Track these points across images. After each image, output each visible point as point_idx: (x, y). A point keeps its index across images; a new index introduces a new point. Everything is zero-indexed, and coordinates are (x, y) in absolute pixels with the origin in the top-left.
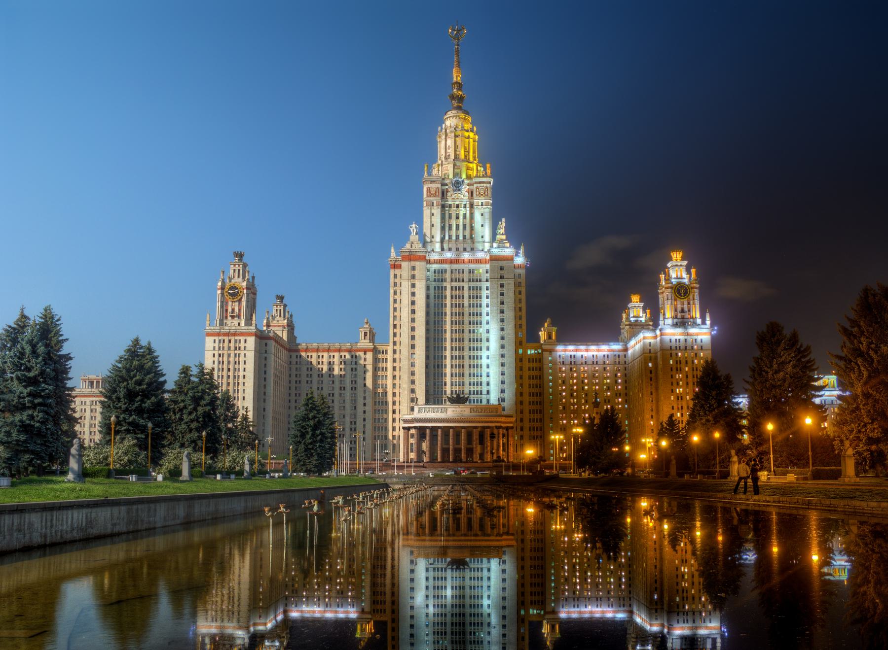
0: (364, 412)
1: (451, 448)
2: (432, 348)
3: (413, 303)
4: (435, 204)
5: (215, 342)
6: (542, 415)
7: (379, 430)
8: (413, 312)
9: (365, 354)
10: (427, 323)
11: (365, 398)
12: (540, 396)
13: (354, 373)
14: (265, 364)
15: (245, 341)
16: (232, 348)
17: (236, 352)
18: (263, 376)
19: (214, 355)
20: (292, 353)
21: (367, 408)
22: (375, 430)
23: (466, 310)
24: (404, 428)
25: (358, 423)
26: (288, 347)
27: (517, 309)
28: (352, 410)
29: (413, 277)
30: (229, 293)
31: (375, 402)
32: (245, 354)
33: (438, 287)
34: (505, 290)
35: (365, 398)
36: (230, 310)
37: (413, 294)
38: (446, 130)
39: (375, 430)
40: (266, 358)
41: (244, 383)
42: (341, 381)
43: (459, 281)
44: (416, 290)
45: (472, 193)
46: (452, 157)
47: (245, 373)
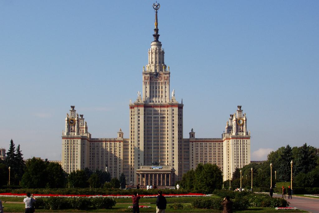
0: (120, 166)
2: (146, 142)
4: (147, 83)
8: (139, 127)
9: (120, 143)
10: (144, 131)
15: (77, 141)
18: (83, 153)
21: (121, 164)
24: (137, 174)
25: (117, 170)
26: (89, 139)
27: (180, 125)
29: (139, 113)
30: (70, 121)
33: (149, 117)
37: (139, 120)
38: (152, 51)
40: (84, 146)
41: (77, 157)
43: (157, 115)
44: (140, 119)
45: (162, 78)
46: (154, 63)
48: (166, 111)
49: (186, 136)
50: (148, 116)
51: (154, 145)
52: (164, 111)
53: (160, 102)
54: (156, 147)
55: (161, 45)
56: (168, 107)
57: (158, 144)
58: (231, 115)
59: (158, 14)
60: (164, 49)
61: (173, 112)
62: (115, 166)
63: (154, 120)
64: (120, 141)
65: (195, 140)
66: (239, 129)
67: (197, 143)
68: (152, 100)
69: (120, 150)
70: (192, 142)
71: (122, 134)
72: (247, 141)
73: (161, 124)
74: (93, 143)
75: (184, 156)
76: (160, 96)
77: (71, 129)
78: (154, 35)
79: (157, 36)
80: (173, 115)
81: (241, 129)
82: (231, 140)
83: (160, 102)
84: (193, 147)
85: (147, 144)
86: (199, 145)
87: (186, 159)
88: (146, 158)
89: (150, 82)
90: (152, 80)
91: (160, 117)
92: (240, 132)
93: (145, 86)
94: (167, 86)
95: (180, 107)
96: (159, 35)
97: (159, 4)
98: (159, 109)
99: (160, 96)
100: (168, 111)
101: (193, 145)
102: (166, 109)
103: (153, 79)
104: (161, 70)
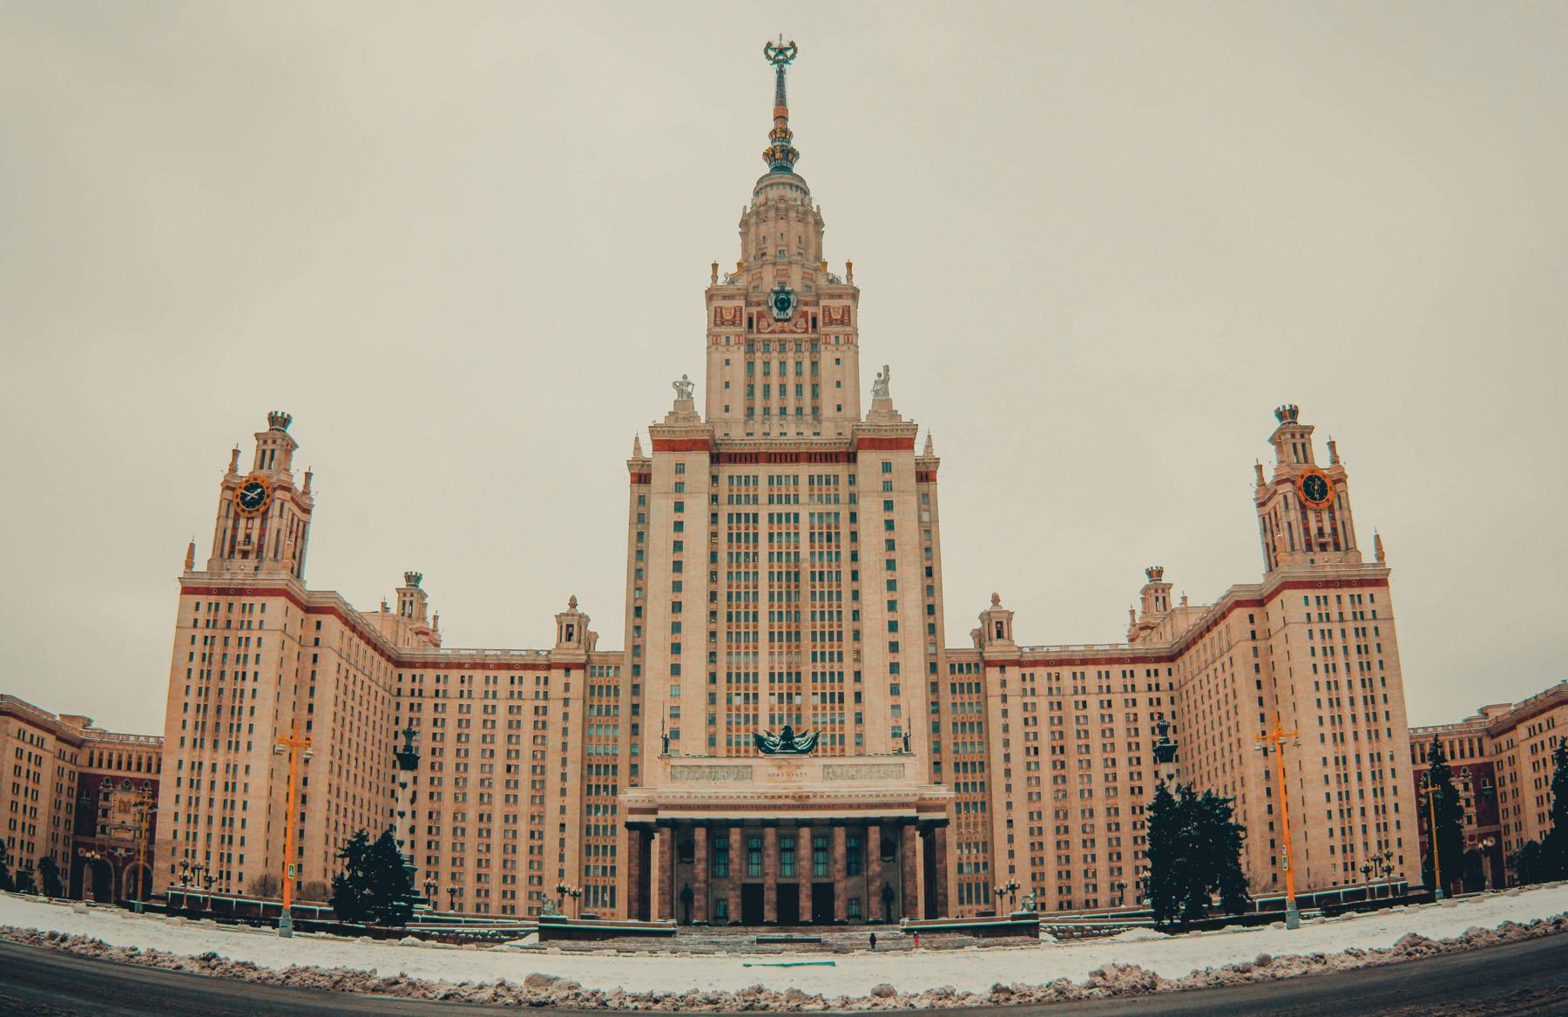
0: (563, 810)
1: (770, 881)
3: (678, 546)
5: (198, 604)
6: (987, 815)
7: (597, 853)
11: (564, 777)
12: (982, 770)
13: (541, 718)
14: (314, 673)
15: (263, 610)
17: (240, 633)
19: (193, 637)
20: (402, 671)
22: (589, 854)
23: (805, 568)
24: (630, 826)
28: (533, 803)
29: (679, 487)
31: (590, 787)
32: (260, 639)
33: (739, 515)
34: (893, 516)
35: (564, 777)
36: (241, 536)
39: (589, 854)
40: (315, 657)
41: (252, 709)
42: (510, 737)
43: (788, 501)
45: (814, 320)
47: (256, 685)
48: (843, 480)
49: (958, 635)
50: (735, 509)
51: (772, 680)
52: (828, 482)
53: (808, 433)
54: (785, 691)
55: (806, 192)
56: (851, 458)
57: (798, 674)
58: (1150, 573)
59: (788, 78)
60: (818, 206)
61: (887, 476)
62: (535, 810)
63: (771, 535)
64: (568, 668)
65: (1015, 656)
66: (1314, 531)
67: (1028, 671)
68: (758, 428)
69: (566, 716)
70: (1002, 665)
71: (584, 619)
72: (1372, 596)
73: (812, 554)
74: (417, 672)
75: (957, 752)
76: (807, 410)
77: (241, 536)
78: (769, 156)
79: (782, 156)
81: (1328, 529)
82: (1273, 607)
84: (1004, 698)
85: (729, 675)
87: (965, 771)
90: (759, 332)
92: (1323, 547)
93: (719, 357)
95: (926, 475)
97: (793, 44)
98: (804, 470)
100: (852, 480)
101: (1004, 684)
102: (841, 470)
103: (764, 323)
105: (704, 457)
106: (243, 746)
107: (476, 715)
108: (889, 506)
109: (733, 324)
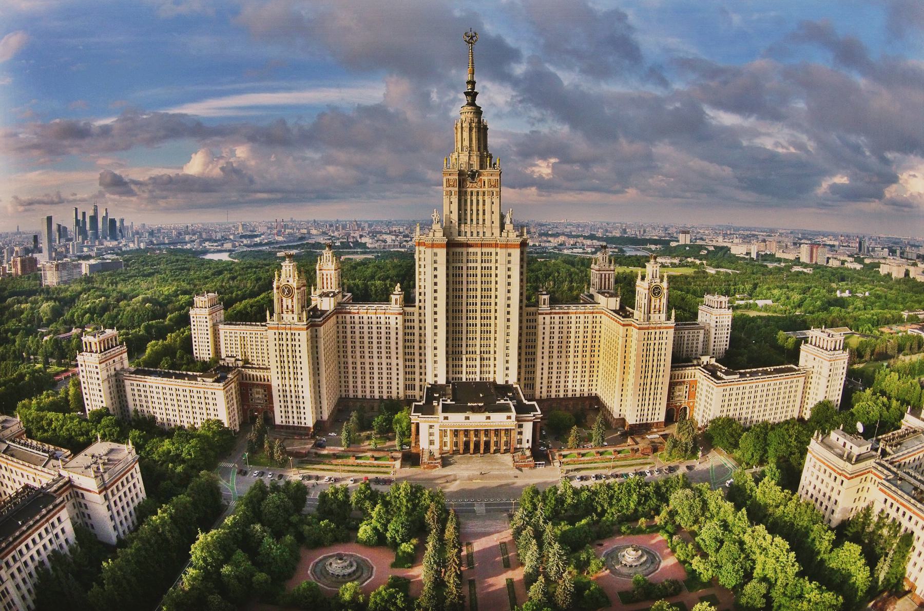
16: (289, 340)
38: (462, 124)
48: (494, 254)
55: (481, 113)
67: (553, 316)
74: (344, 315)
76: (481, 222)
78: (467, 94)
79: (472, 95)
80: (509, 266)
81: (657, 307)
83: (481, 234)
86: (557, 320)
88: (450, 352)
89: (460, 192)
91: (479, 268)
94: (496, 200)
96: (476, 93)
98: (478, 250)
99: (481, 222)
100: (497, 254)
102: (493, 250)
104: (481, 167)
105: (444, 251)
106: (300, 379)
107: (366, 330)
108: (509, 269)
109: (453, 186)
